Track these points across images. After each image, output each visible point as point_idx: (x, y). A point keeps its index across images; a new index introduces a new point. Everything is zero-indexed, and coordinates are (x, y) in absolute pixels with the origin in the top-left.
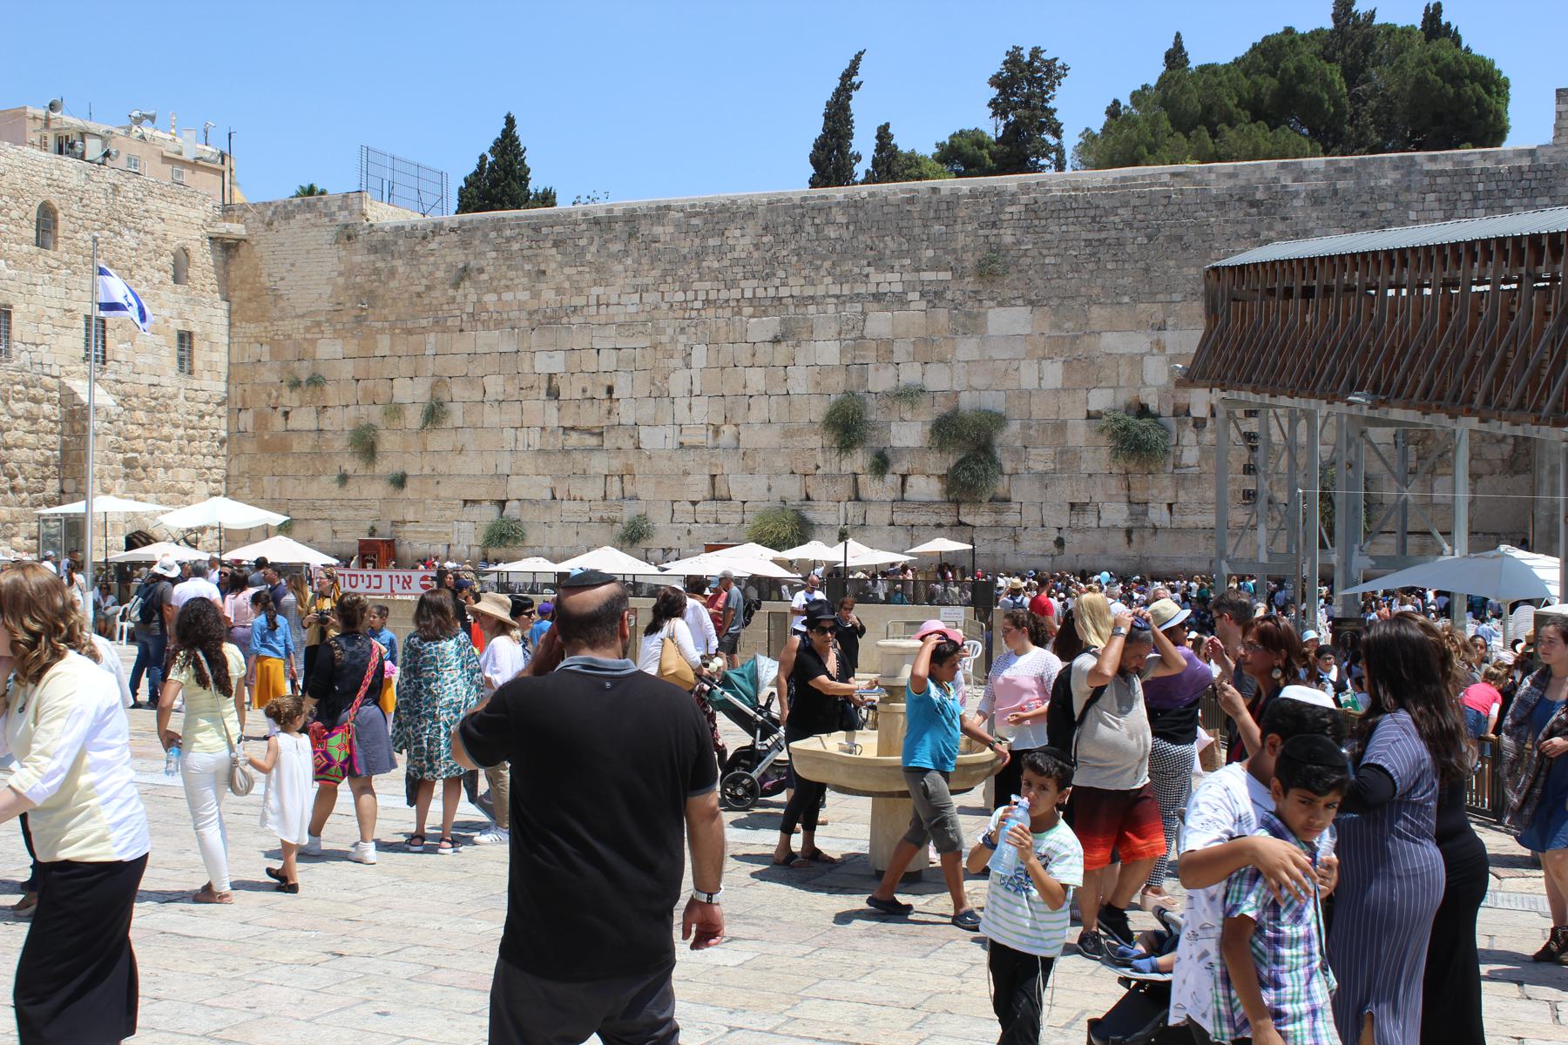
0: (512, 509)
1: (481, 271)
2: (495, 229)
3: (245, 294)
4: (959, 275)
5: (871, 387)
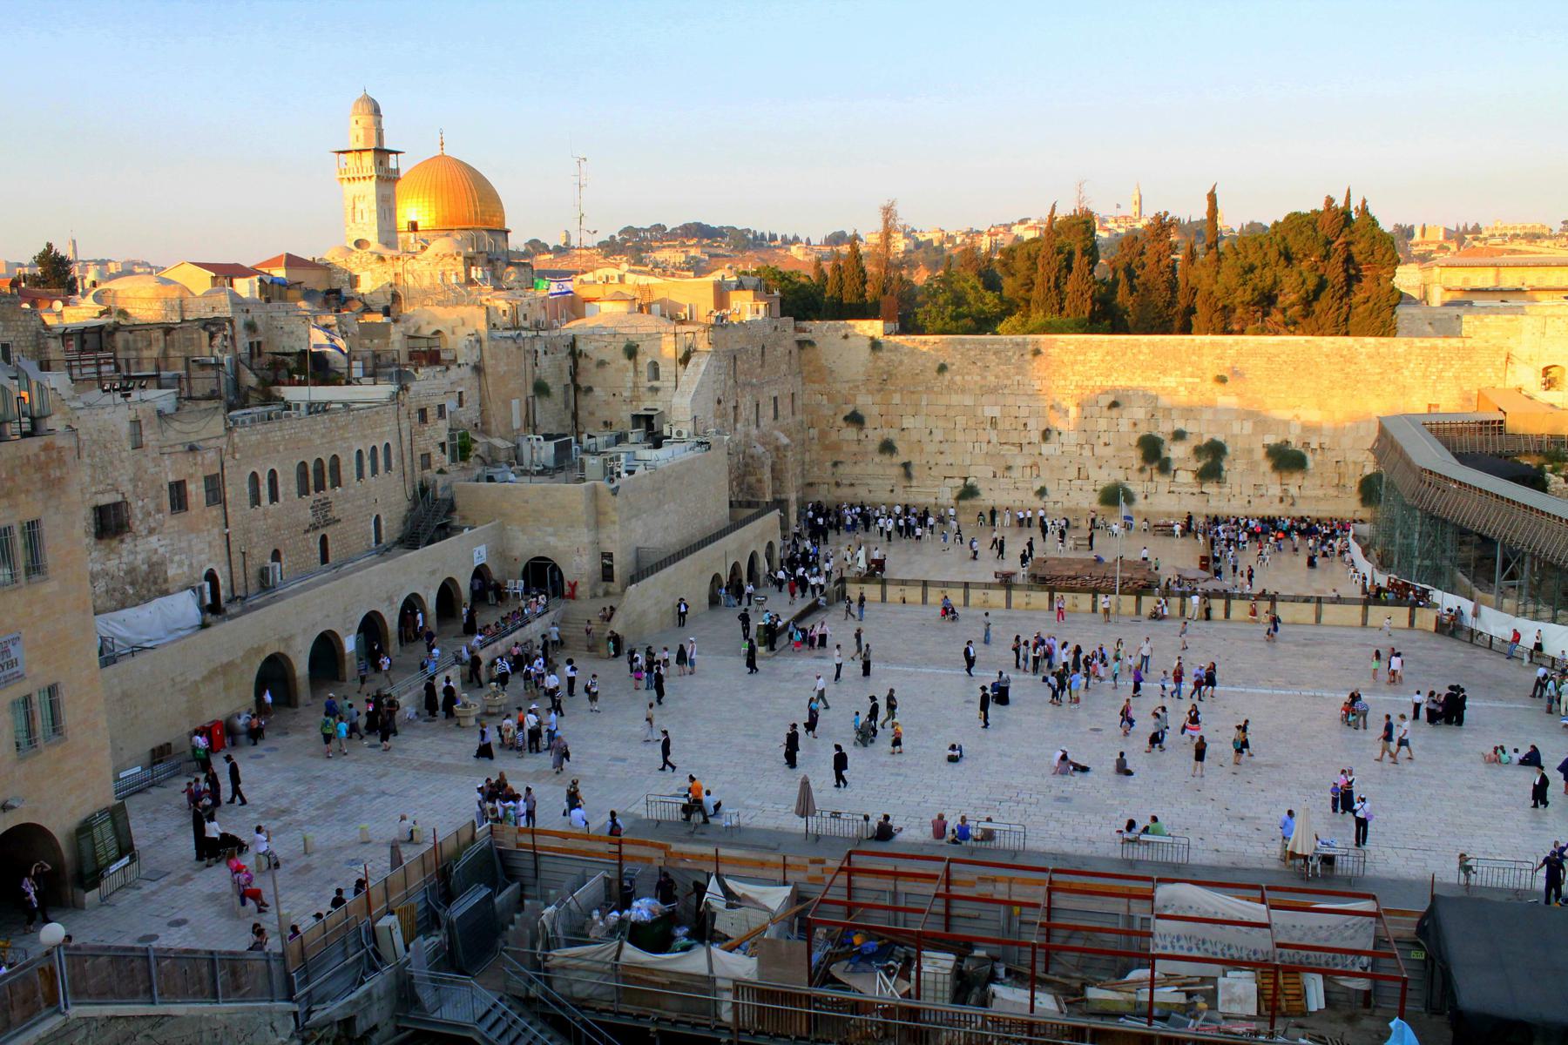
4: (1203, 380)
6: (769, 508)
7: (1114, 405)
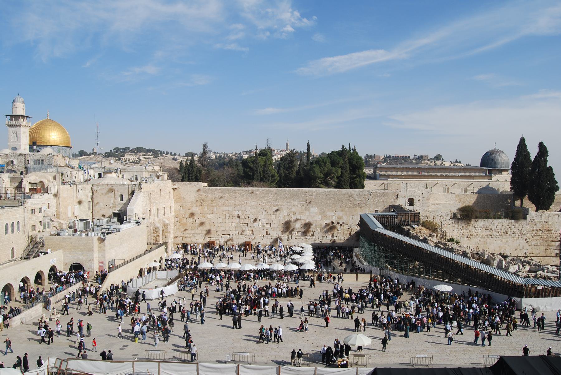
0: (231, 236)
1: (225, 197)
2: (227, 190)
3: (177, 198)
6: (161, 245)
7: (277, 210)
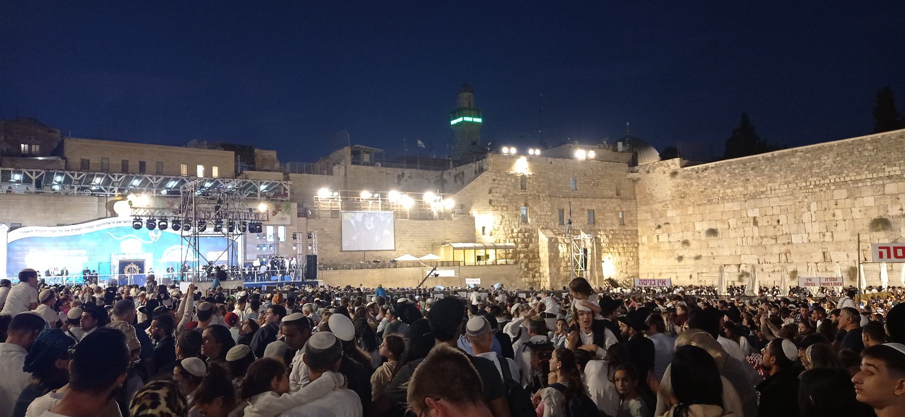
1: (725, 181)
5: (890, 213)
